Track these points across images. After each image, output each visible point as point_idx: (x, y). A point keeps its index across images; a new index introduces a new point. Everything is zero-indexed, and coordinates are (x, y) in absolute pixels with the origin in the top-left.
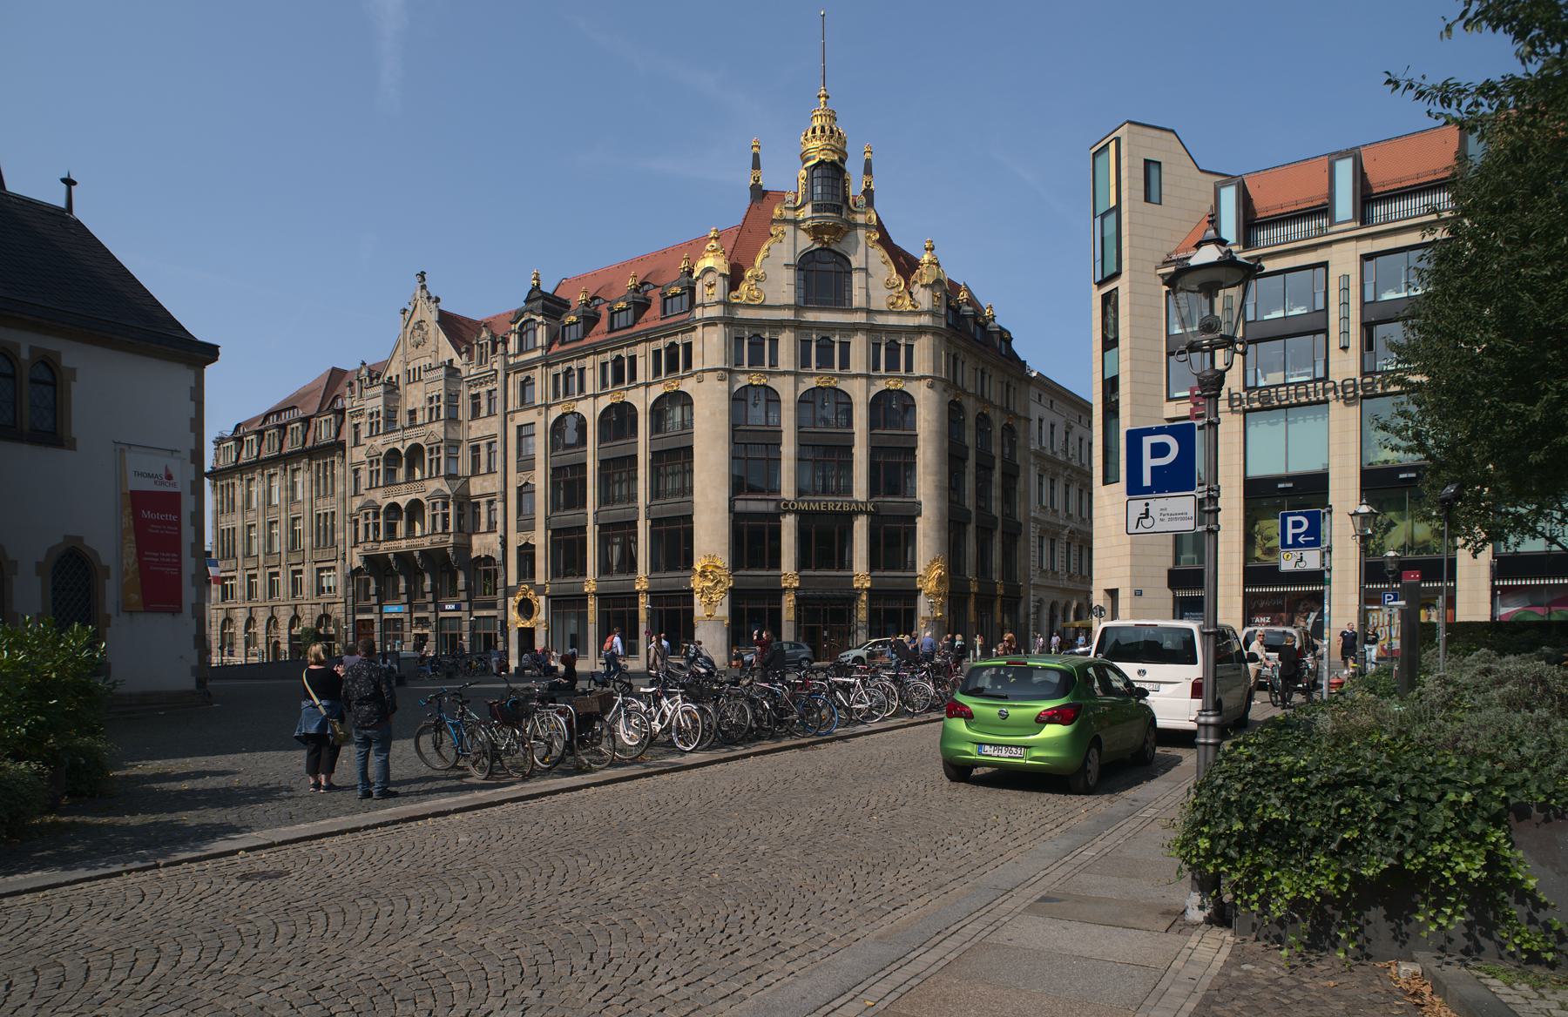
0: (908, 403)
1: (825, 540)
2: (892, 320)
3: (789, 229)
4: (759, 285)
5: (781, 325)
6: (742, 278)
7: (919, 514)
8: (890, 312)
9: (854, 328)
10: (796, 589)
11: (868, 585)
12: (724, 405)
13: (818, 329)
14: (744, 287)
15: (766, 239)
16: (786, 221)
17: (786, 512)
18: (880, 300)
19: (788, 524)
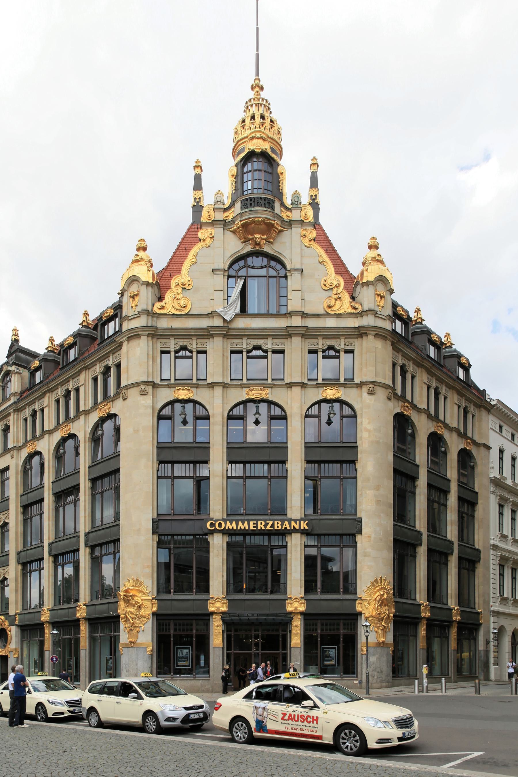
1: (255, 564)
2: (331, 323)
3: (218, 231)
4: (186, 293)
5: (207, 334)
6: (169, 288)
7: (360, 532)
9: (288, 333)
10: (223, 613)
11: (302, 608)
12: (148, 420)
13: (249, 337)
14: (168, 297)
15: (195, 243)
16: (213, 223)
17: (212, 532)
19: (218, 545)
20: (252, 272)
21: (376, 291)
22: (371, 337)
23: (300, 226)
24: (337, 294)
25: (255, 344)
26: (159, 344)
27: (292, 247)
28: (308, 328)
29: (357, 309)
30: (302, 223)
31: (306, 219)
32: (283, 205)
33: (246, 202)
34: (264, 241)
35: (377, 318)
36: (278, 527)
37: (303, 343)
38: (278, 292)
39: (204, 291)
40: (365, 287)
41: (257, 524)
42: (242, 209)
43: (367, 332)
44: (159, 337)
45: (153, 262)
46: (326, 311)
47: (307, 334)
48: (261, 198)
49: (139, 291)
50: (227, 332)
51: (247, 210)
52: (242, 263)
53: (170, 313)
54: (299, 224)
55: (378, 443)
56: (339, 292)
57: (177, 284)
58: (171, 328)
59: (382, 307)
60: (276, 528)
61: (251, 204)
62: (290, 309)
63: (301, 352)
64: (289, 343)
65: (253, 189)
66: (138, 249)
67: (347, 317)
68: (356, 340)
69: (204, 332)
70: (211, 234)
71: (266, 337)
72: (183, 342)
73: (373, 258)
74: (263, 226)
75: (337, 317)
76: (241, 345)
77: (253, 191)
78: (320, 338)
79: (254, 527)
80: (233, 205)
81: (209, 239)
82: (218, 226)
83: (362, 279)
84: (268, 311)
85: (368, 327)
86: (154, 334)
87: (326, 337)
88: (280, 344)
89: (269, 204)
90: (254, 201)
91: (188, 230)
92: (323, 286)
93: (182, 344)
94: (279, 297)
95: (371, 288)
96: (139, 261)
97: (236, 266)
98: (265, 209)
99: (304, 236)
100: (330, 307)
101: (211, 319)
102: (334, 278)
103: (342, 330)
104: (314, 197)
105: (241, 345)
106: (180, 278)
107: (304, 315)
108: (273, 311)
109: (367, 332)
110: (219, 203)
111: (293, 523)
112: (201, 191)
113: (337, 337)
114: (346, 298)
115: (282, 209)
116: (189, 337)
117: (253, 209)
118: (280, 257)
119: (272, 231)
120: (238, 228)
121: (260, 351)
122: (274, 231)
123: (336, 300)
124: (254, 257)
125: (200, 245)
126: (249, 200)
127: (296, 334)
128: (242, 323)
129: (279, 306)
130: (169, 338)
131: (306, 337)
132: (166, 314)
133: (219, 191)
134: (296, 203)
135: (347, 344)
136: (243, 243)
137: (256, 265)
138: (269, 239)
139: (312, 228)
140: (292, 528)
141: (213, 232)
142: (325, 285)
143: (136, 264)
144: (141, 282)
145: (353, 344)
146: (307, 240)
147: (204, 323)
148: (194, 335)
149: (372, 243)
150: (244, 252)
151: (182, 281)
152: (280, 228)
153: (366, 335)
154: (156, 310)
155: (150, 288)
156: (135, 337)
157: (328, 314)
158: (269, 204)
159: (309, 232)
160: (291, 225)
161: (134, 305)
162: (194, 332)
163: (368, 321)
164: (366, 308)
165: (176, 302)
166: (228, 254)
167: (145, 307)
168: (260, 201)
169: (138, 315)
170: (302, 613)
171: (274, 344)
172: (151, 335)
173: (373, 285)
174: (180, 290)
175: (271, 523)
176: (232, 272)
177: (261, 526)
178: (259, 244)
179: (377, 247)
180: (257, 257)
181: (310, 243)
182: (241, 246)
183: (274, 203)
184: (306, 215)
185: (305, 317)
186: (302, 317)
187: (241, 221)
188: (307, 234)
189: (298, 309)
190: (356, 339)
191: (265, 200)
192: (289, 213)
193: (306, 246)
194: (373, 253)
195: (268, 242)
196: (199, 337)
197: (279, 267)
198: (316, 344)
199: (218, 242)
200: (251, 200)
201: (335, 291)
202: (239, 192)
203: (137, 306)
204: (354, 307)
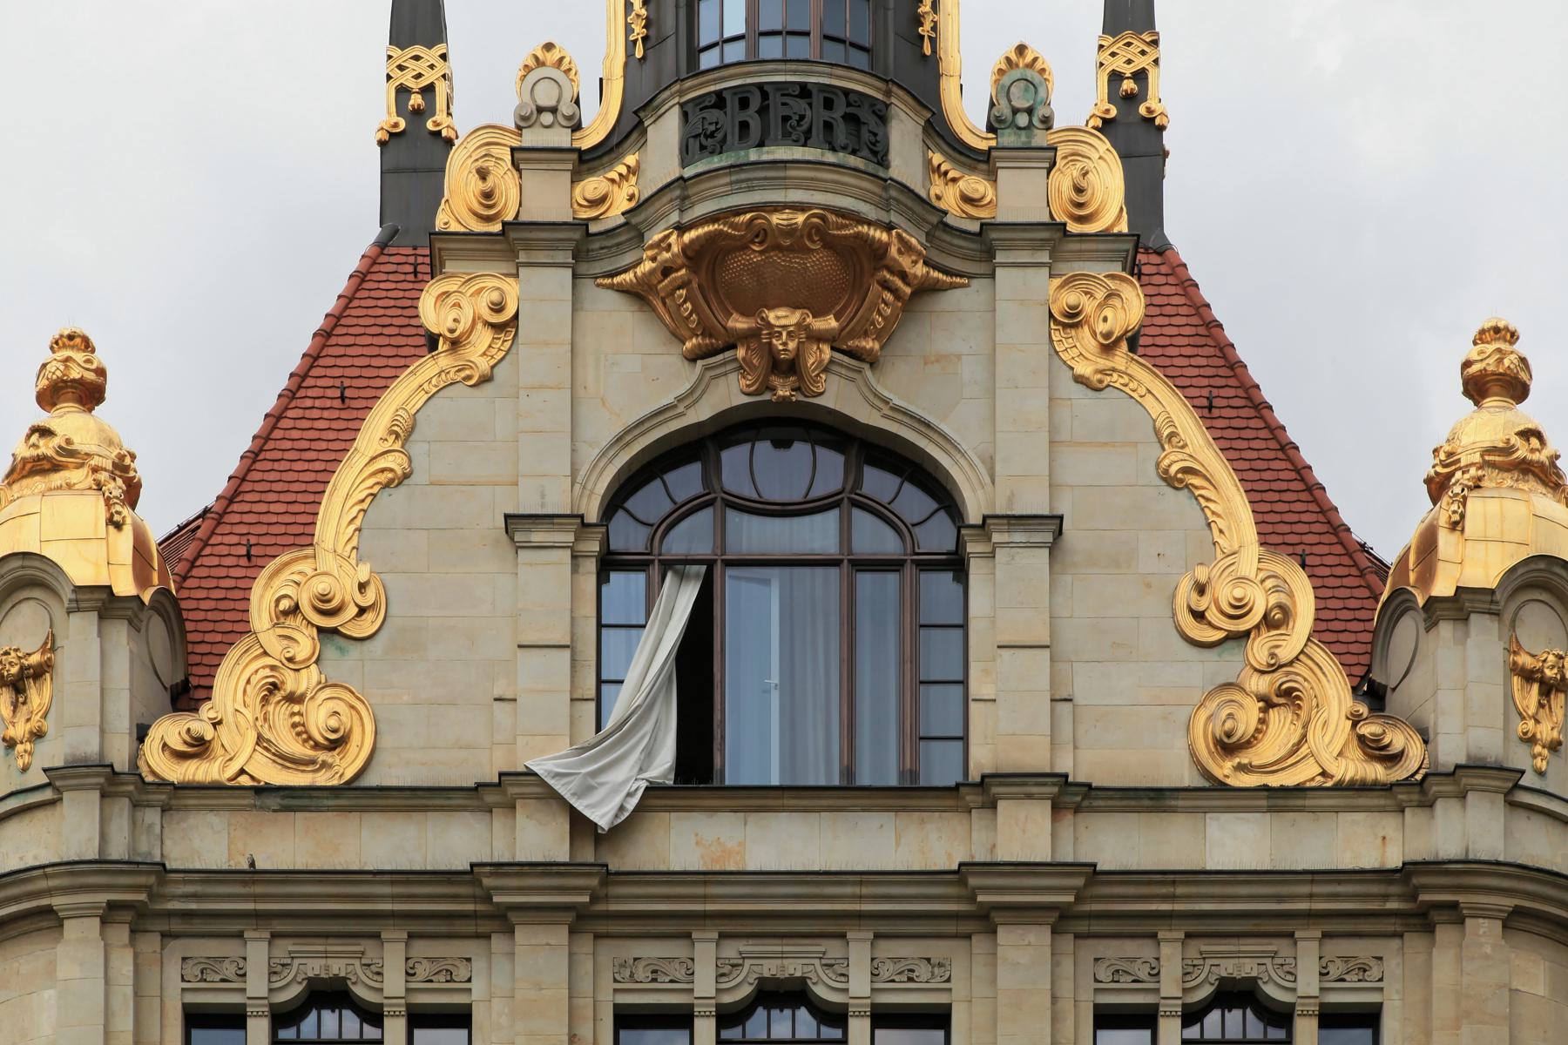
2: (1235, 843)
3: (539, 291)
4: (344, 664)
5: (474, 907)
8: (1213, 794)
13: (732, 926)
14: (234, 684)
15: (400, 363)
16: (512, 241)
18: (1146, 721)
20: (752, 535)
21: (1514, 648)
22: (1484, 932)
23: (1044, 257)
24: (1274, 668)
25: (770, 969)
26: (173, 971)
27: (997, 384)
28: (1092, 873)
29: (1394, 759)
30: (1054, 239)
31: (1081, 220)
32: (938, 130)
33: (714, 114)
34: (826, 349)
35: (1523, 814)
37: (1067, 965)
38: (911, 657)
39: (454, 655)
40: (1445, 629)
42: (686, 156)
43: (1461, 898)
44: (176, 926)
45: (142, 469)
46: (1206, 774)
47: (1085, 908)
48: (804, 91)
49: (50, 645)
50: (595, 895)
51: (716, 162)
52: (686, 481)
53: (244, 781)
54: (1037, 245)
56: (1285, 654)
57: (285, 605)
58: (253, 874)
59: (1554, 747)
61: (744, 126)
62: (983, 758)
63: (1055, 1020)
64: (979, 970)
65: (755, 33)
66: (50, 396)
67: (1336, 810)
68: (1389, 947)
69: (454, 898)
70: (498, 308)
71: (835, 926)
72: (326, 955)
73: (1493, 450)
74: (818, 261)
75: (1271, 809)
76: (680, 974)
77: (753, 48)
78: (1171, 935)
80: (631, 128)
81: (483, 337)
82: (542, 257)
83: (1427, 576)
84: (849, 771)
85: (1467, 870)
86: (145, 904)
87: (1202, 928)
88: (923, 971)
89: (855, 127)
90: (763, 111)
91: (360, 278)
93: (315, 968)
94: (916, 683)
95: (1484, 636)
96: (56, 468)
97: (651, 501)
98: (830, 157)
99: (1073, 319)
100: (1228, 746)
101: (499, 821)
102: (1248, 570)
103: (1305, 889)
104: (1128, 85)
105: (680, 974)
106: (306, 567)
107: (1072, 797)
108: (880, 768)
109: (1461, 898)
110: (547, 118)
112: (439, 49)
113: (1276, 926)
114: (1333, 693)
115: (937, 158)
116: (361, 927)
117: (753, 155)
118: (922, 443)
119: (876, 287)
120: (666, 271)
121: (803, 1013)
122: (886, 285)
123: (1268, 704)
124: (764, 448)
125: (428, 370)
126: (732, 103)
127: (1023, 913)
128: (688, 842)
129: (916, 738)
130: (239, 935)
131: (1082, 927)
132: (216, 787)
133: (549, 47)
134: (1022, 120)
135: (1335, 971)
136: (692, 358)
137: (775, 492)
138: (853, 335)
139: (1116, 269)
141: (512, 291)
142: (1199, 616)
143: (38, 483)
144: (67, 594)
145: (1375, 973)
146: (1086, 341)
147: (453, 843)
148: (392, 915)
149: (1486, 359)
150: (703, 412)
151: (321, 586)
152: (920, 270)
153: (1455, 914)
154: (158, 763)
155: (120, 633)
156: (25, 925)
157: (1220, 787)
158: (855, 127)
159: (1100, 294)
160: (989, 254)
161: (19, 730)
162: (394, 898)
163: (1466, 830)
164: (1451, 751)
165: (280, 714)
166: (603, 426)
167: (90, 746)
168: (799, 106)
169: (48, 795)
171: (887, 971)
172: (128, 916)
173: (1497, 614)
174: (305, 644)
176: (628, 536)
178: (791, 367)
179: (1516, 388)
180: (782, 444)
181: (1103, 363)
182: (684, 377)
183: (883, 119)
184: (1079, 190)
185: (1077, 810)
186: (1057, 809)
187: (681, 229)
188: (1089, 306)
189: (1036, 759)
190: (1396, 943)
191: (829, 104)
192: (974, 184)
193: (1080, 380)
194: (1492, 424)
195: (850, 353)
196: (420, 926)
197: (914, 503)
198: (1143, 973)
199: (539, 356)
200: (744, 104)
201: (1259, 650)
202: (670, 54)
203: (37, 735)
204: (1375, 750)
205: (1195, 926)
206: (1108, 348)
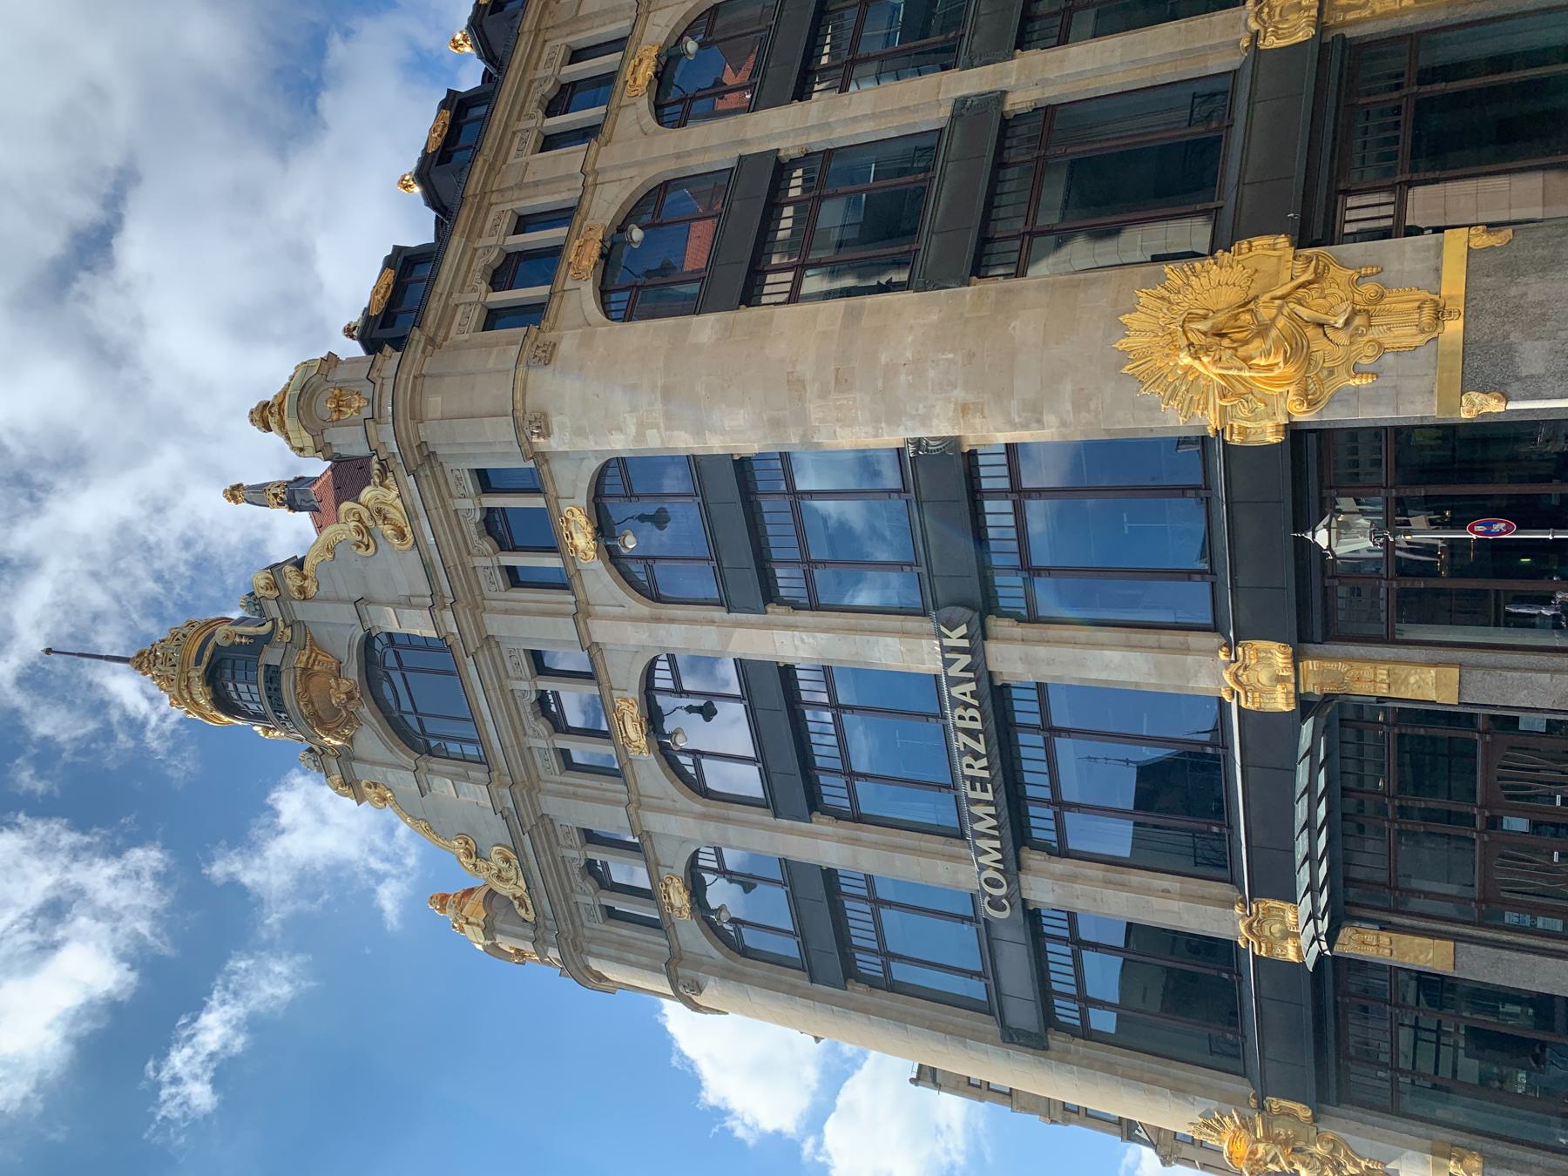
0: (616, 485)
36: (973, 719)
41: (973, 779)
55: (667, 394)
60: (978, 726)
79: (984, 790)
92: (372, 548)
111: (954, 671)
140: (971, 675)
170: (1296, 659)
175: (963, 738)
177: (979, 769)
205: (464, 553)
206: (305, 578)
